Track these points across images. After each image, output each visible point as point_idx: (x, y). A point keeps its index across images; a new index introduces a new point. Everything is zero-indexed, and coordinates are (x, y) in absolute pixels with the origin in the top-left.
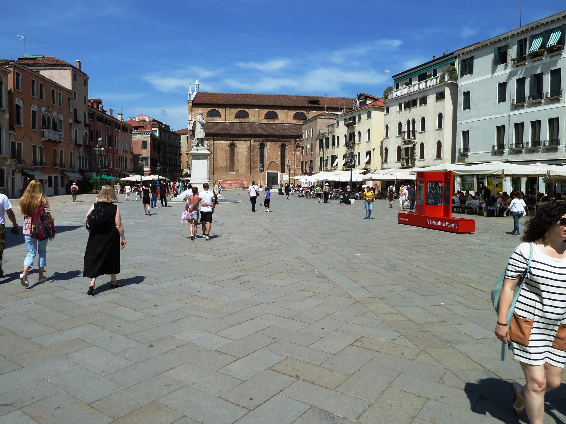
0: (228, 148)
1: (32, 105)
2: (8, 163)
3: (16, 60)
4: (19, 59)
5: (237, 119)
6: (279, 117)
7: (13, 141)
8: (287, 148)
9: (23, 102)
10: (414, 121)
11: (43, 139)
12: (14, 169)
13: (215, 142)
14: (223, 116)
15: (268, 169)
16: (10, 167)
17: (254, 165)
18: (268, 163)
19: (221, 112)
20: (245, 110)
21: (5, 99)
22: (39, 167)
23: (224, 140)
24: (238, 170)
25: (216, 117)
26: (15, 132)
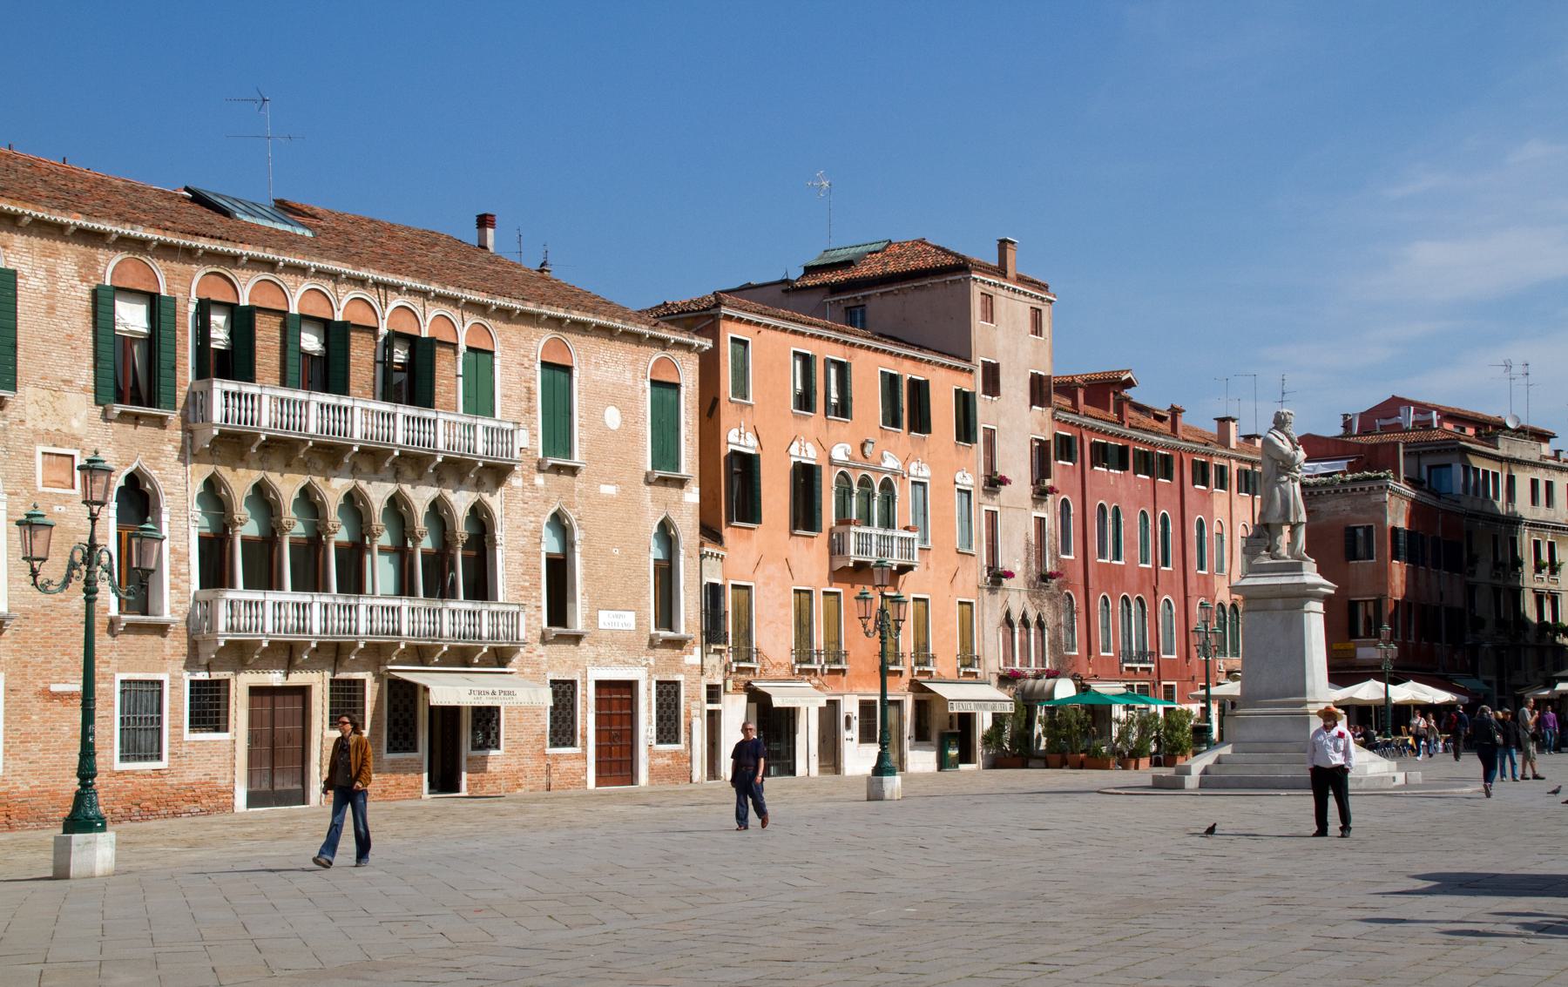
1: (796, 444)
2: (693, 657)
3: (795, 273)
4: (810, 270)
7: (719, 581)
9: (758, 439)
11: (839, 565)
12: (719, 681)
16: (702, 672)
21: (688, 440)
22: (819, 667)
26: (725, 550)
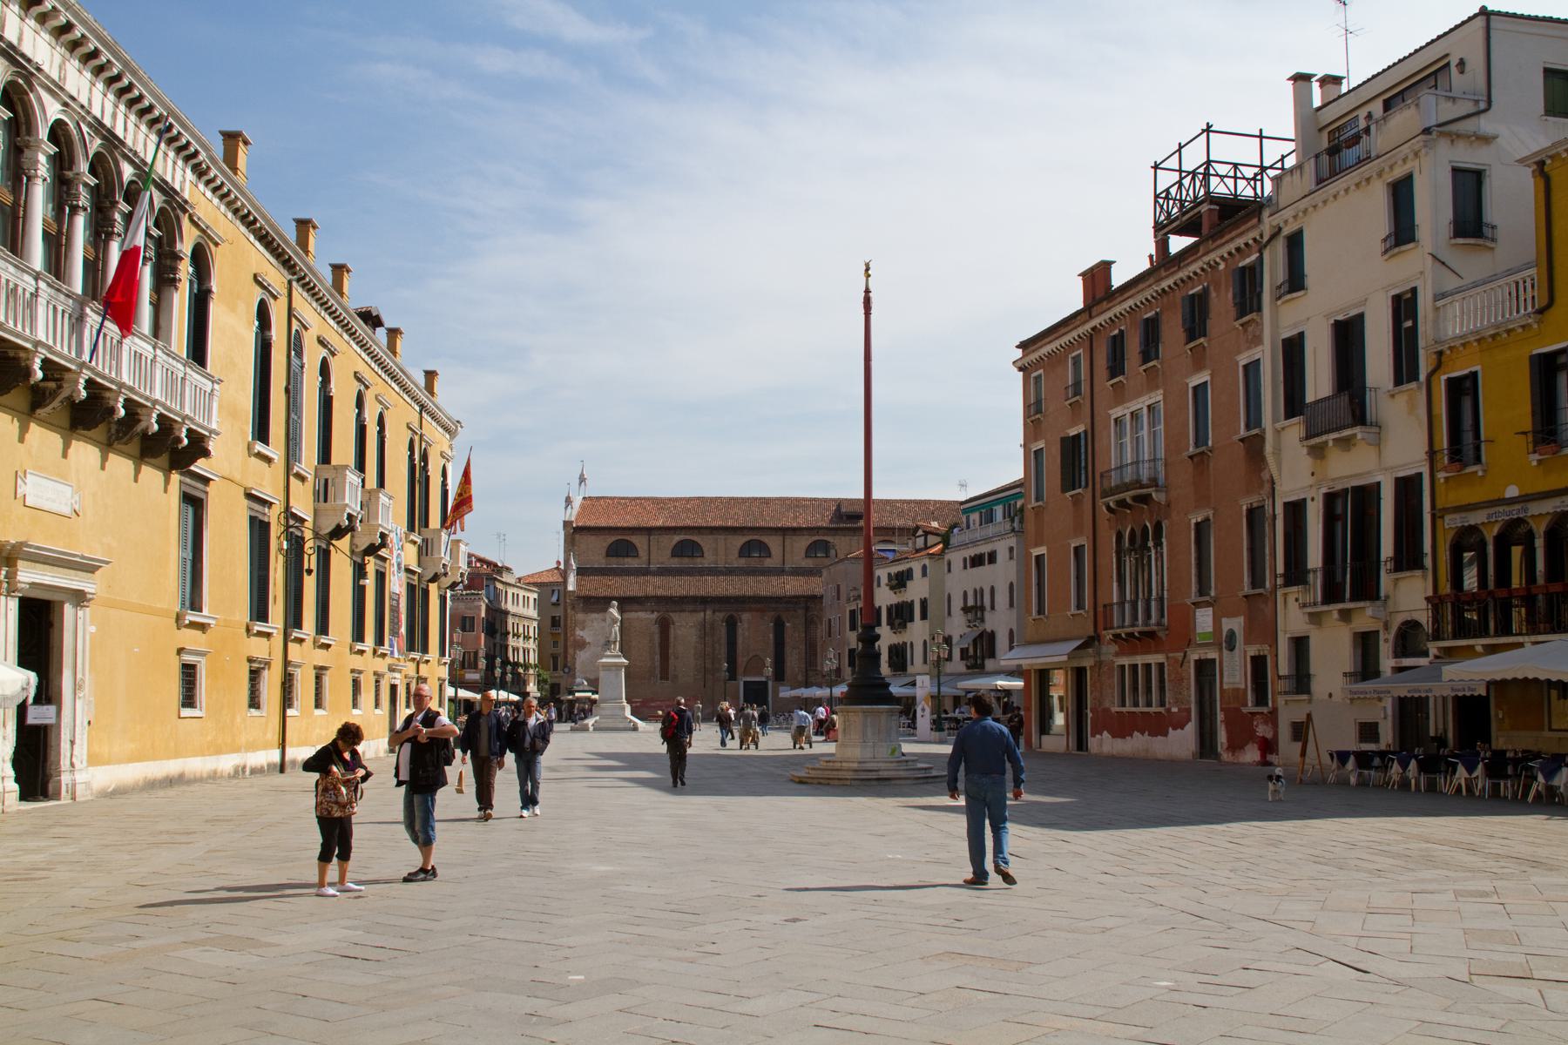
0: (655, 629)
5: (676, 560)
6: (773, 553)
8: (788, 624)
10: (982, 590)
13: (626, 615)
14: (643, 553)
15: (745, 673)
17: (713, 663)
18: (745, 659)
19: (638, 545)
20: (695, 538)
23: (646, 611)
24: (676, 677)
25: (627, 556)
